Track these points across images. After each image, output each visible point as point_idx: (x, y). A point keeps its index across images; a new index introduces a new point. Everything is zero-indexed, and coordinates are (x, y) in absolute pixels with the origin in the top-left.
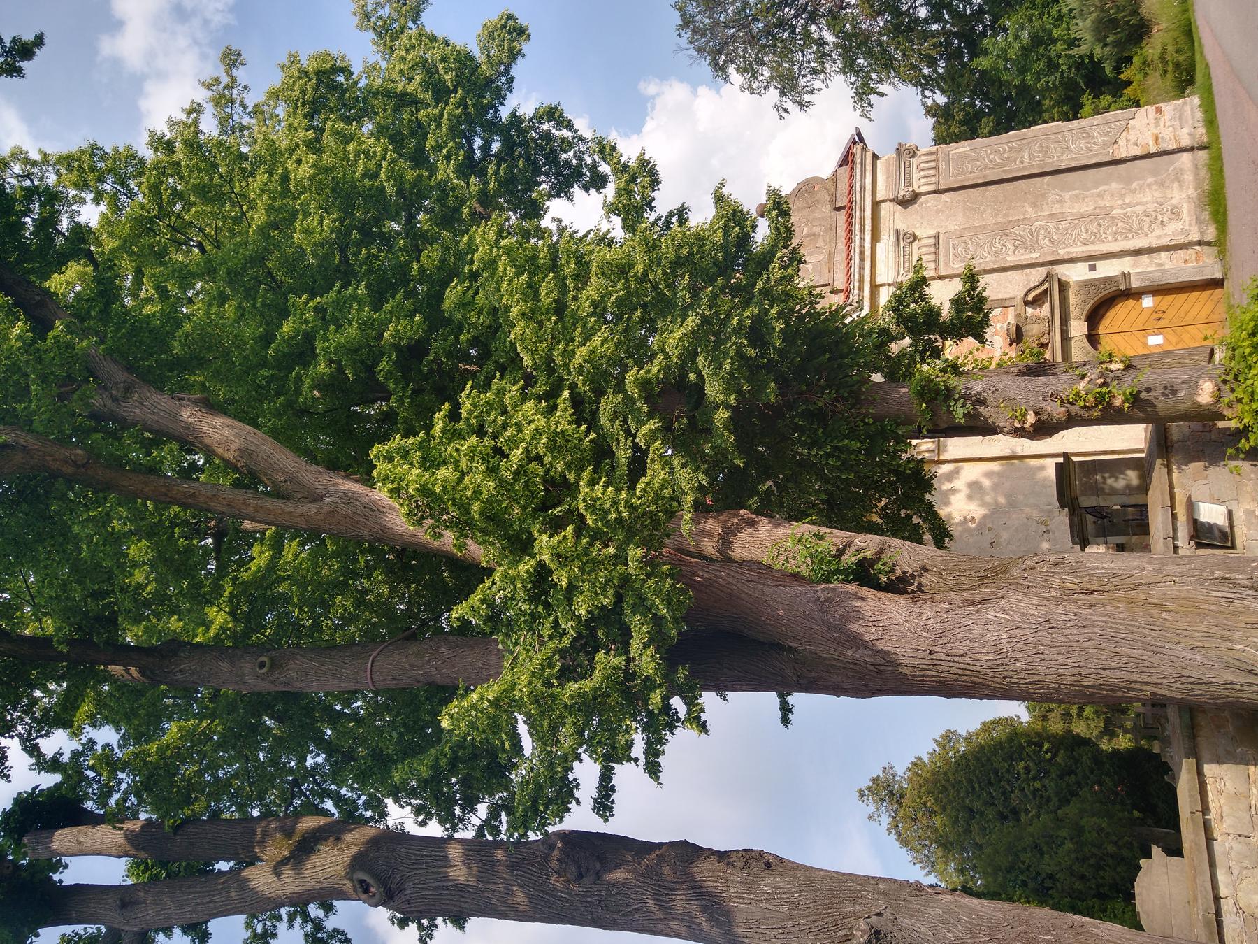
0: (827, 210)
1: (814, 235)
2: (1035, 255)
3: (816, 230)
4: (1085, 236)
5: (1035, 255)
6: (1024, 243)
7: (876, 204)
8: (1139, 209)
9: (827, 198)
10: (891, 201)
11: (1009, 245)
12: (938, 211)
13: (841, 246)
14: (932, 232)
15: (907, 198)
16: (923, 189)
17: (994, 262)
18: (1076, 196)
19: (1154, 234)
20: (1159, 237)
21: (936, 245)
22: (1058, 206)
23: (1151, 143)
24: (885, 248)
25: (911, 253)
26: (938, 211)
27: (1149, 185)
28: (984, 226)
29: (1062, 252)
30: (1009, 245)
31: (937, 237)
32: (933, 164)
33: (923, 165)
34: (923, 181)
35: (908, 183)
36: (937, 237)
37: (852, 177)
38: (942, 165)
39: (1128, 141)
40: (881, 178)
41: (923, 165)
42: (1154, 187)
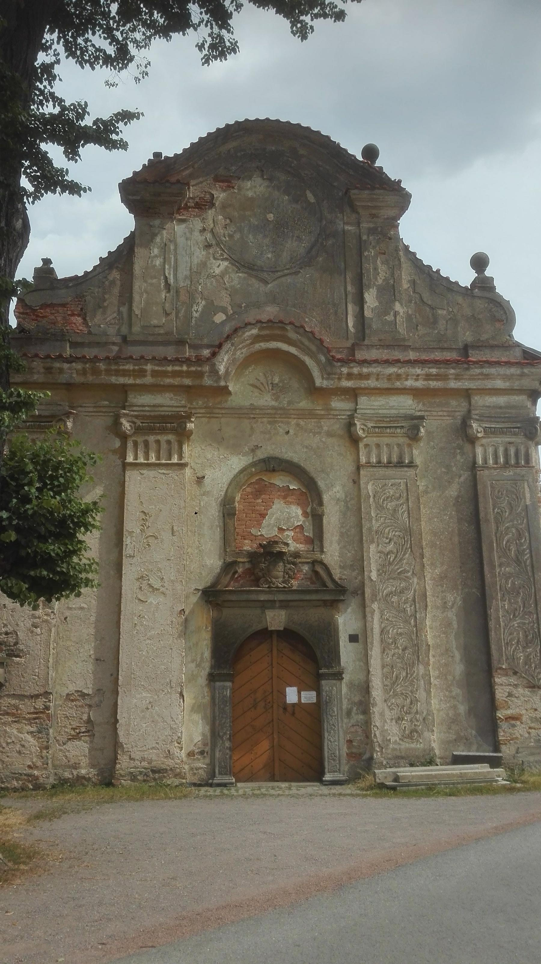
0: (467, 336)
1: (435, 322)
2: (374, 575)
3: (441, 325)
4: (392, 632)
5: (374, 575)
6: (390, 564)
7: (467, 394)
8: (421, 694)
9: (484, 337)
10: (469, 411)
11: (391, 547)
12: (448, 467)
13: (412, 355)
14: (418, 461)
15: (469, 431)
16: (479, 451)
17: (370, 529)
18: (449, 625)
19: (386, 709)
20: (382, 714)
21: (400, 464)
22: (439, 602)
23: (509, 712)
24: (406, 404)
25: (393, 435)
26: (448, 467)
27: (455, 707)
28: (419, 520)
29: (375, 606)
30: (391, 547)
31: (411, 465)
32: (513, 462)
33: (512, 451)
34: (491, 450)
35: (488, 432)
36: (411, 465)
37: (508, 364)
38: (509, 473)
39: (516, 686)
40: (502, 400)
41: (512, 451)
42: (451, 713)
